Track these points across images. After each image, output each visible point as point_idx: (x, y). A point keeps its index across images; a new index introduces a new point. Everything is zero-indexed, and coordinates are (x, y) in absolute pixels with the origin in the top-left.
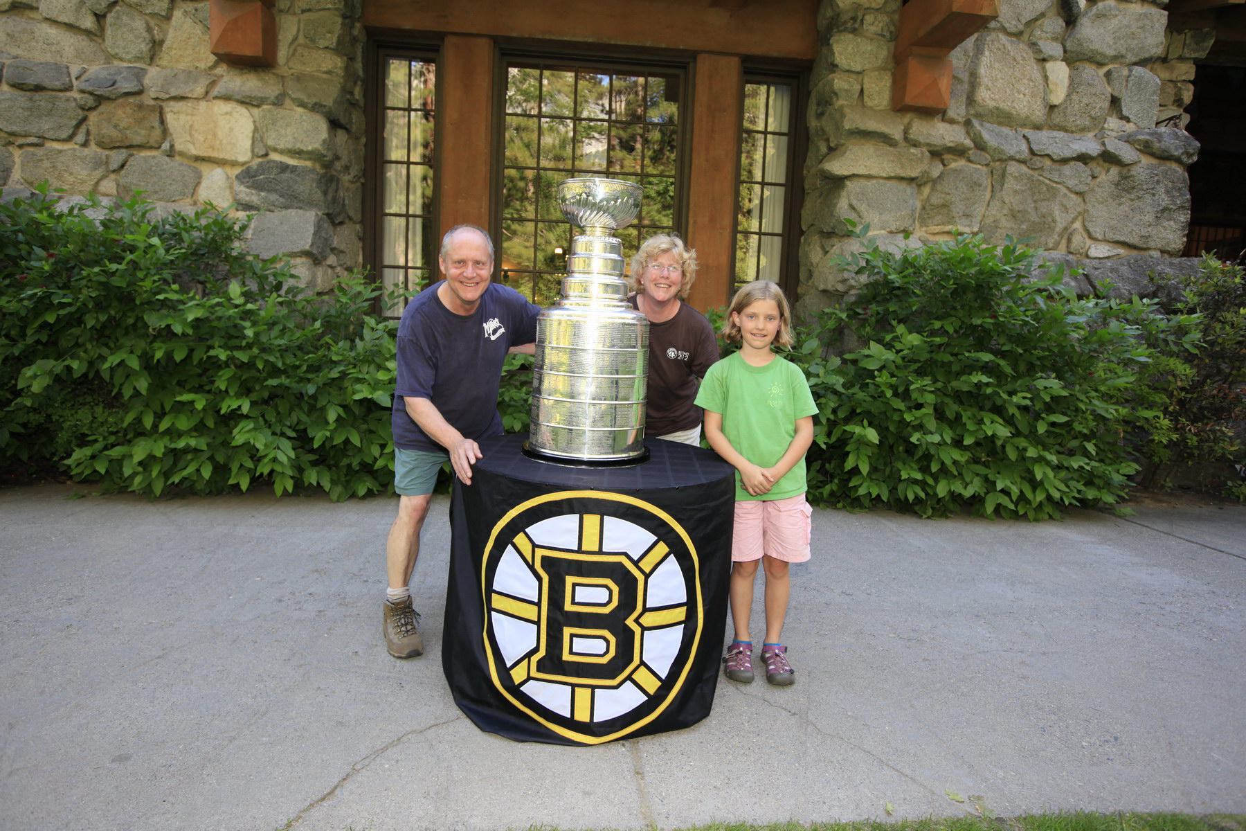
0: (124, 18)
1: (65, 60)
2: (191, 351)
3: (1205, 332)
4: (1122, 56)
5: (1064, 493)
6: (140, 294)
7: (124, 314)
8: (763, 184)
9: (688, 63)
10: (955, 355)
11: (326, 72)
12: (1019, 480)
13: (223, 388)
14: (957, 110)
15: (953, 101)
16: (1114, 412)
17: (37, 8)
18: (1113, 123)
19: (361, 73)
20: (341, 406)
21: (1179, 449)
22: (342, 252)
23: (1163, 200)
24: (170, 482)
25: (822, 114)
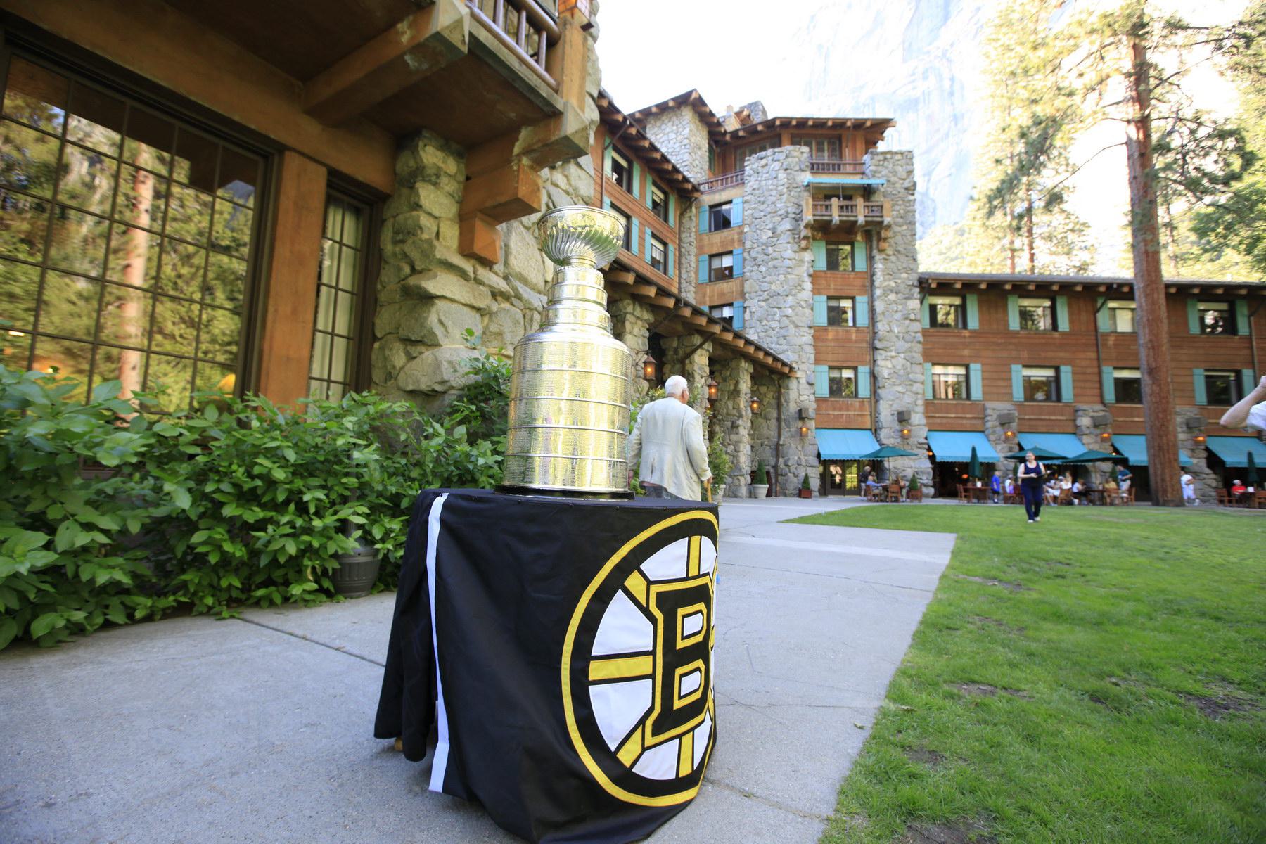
14: (499, 267)
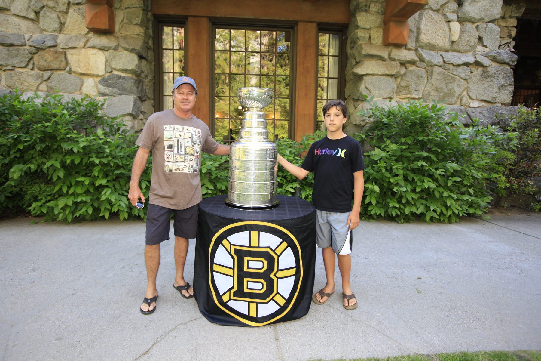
0: (48, 13)
1: (22, 32)
2: (82, 159)
3: (520, 139)
4: (483, 19)
5: (460, 210)
6: (59, 135)
7: (52, 144)
8: (328, 78)
9: (294, 26)
10: (413, 153)
11: (136, 35)
12: (440, 206)
13: (97, 175)
14: (411, 44)
15: (409, 41)
16: (480, 176)
17: (9, 10)
18: (479, 48)
19: (151, 34)
20: (147, 181)
21: (510, 191)
22: (146, 113)
23: (502, 81)
24: (74, 216)
25: (353, 47)
